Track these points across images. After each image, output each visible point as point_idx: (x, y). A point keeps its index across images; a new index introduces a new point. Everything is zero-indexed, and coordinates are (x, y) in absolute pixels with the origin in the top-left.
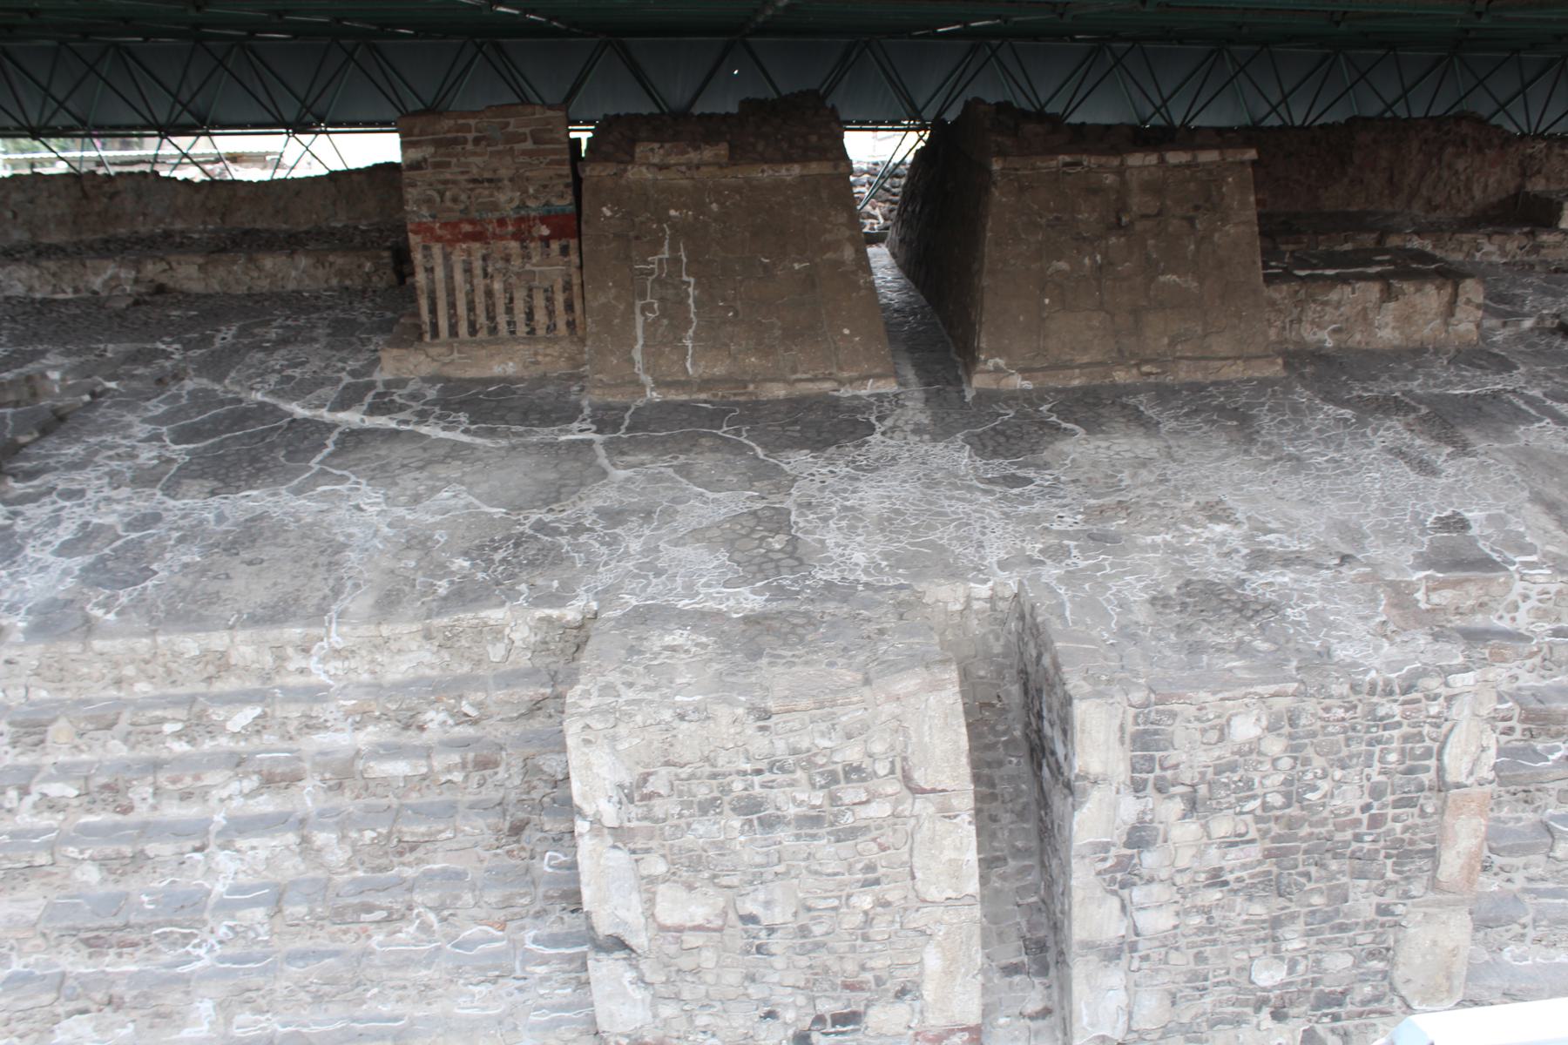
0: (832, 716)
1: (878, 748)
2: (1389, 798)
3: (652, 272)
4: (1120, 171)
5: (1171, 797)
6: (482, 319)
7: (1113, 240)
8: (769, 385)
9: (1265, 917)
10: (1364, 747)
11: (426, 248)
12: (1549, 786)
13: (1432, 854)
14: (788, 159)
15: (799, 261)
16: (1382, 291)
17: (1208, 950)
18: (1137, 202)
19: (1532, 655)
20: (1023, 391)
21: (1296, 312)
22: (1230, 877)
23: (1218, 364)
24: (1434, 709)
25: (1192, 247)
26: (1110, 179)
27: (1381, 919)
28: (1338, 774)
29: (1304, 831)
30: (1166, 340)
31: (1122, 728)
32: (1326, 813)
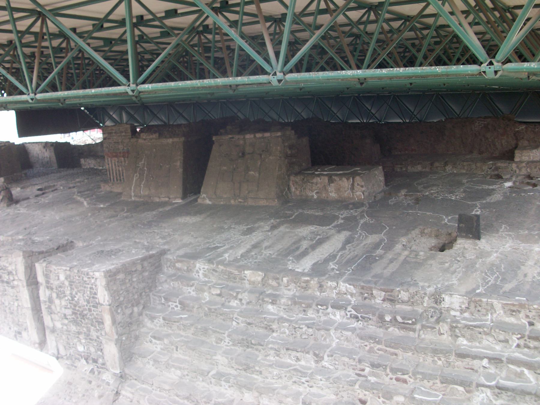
0: (8, 259)
2: (92, 304)
3: (139, 167)
5: (54, 292)
6: (118, 178)
7: (240, 161)
8: (155, 198)
9: (77, 331)
10: (83, 288)
11: (108, 159)
13: (103, 323)
14: (171, 137)
15: (168, 165)
17: (69, 337)
18: (248, 149)
19: (192, 286)
20: (209, 204)
21: (304, 185)
25: (259, 163)
26: (241, 142)
27: (98, 340)
28: (79, 294)
29: (77, 308)
30: (247, 192)
31: (43, 272)
32: (80, 305)
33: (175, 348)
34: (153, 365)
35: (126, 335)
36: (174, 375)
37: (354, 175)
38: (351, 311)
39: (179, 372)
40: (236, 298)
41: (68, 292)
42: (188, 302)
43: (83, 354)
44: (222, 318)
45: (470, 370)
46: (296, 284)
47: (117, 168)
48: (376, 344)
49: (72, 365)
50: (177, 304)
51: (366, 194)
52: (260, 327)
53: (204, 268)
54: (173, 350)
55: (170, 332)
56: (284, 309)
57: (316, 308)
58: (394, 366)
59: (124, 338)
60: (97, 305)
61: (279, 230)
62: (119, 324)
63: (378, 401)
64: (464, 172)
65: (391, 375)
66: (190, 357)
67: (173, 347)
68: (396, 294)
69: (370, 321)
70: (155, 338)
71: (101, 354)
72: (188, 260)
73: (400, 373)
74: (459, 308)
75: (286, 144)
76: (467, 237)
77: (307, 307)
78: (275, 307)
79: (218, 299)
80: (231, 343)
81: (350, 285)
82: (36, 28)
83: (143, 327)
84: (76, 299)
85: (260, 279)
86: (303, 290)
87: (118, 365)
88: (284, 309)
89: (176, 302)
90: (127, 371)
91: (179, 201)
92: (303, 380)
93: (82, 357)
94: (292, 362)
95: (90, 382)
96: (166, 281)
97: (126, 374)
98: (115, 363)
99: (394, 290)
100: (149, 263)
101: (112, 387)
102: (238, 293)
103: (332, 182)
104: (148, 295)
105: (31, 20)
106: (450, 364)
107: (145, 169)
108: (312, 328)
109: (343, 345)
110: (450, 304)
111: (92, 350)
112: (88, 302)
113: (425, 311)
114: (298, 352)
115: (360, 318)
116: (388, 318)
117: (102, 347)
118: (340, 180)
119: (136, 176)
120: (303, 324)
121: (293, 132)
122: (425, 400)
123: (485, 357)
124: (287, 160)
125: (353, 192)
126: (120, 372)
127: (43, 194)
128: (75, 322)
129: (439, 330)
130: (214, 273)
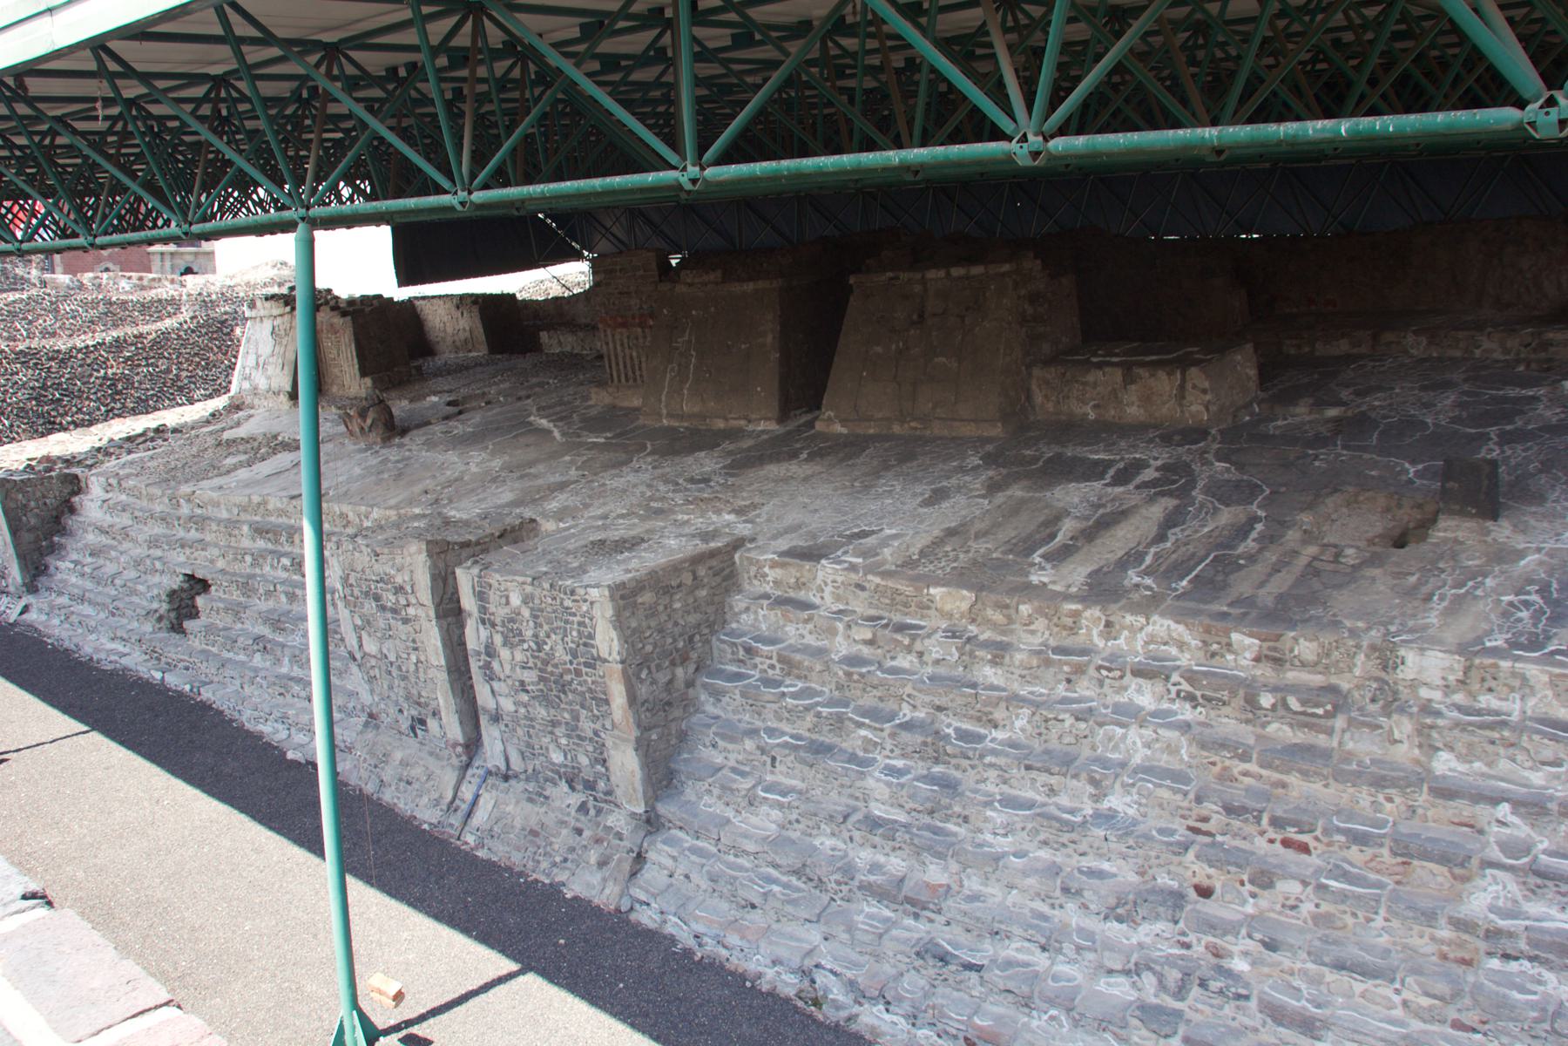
1: (407, 579)
3: (677, 349)
4: (923, 282)
6: (630, 373)
12: (768, 705)
13: (607, 702)
14: (750, 279)
16: (1124, 376)
19: (806, 621)
20: (841, 434)
22: (529, 688)
23: (957, 424)
24: (585, 608)
26: (918, 288)
28: (553, 636)
29: (550, 669)
30: (930, 405)
32: (556, 661)
33: (769, 761)
34: (720, 798)
35: (659, 730)
36: (765, 821)
37: (1184, 363)
38: (1179, 684)
39: (776, 814)
40: (909, 649)
41: (529, 633)
42: (798, 657)
43: (562, 770)
44: (878, 694)
45: (1465, 829)
46: (1050, 620)
47: (627, 351)
48: (1236, 762)
49: (540, 795)
50: (774, 661)
51: (1213, 408)
52: (965, 716)
53: (834, 581)
54: (764, 764)
55: (759, 724)
56: (1023, 677)
57: (1096, 674)
58: (1279, 813)
59: (654, 737)
60: (594, 662)
61: (1009, 493)
62: (643, 704)
63: (1239, 892)
64: (1458, 354)
65: (1271, 834)
66: (803, 781)
67: (764, 757)
68: (1288, 645)
69: (1226, 710)
70: (724, 737)
71: (603, 770)
72: (798, 561)
73: (1293, 830)
74: (1441, 683)
75: (1023, 292)
76: (1462, 513)
77: (1075, 673)
78: (1000, 672)
79: (866, 651)
80: (897, 751)
81: (1178, 622)
82: (463, 39)
83: (697, 711)
84: (547, 648)
85: (965, 606)
86: (1065, 633)
87: (640, 795)
88: (1023, 677)
89: (771, 658)
90: (662, 808)
91: (772, 426)
92: (1065, 838)
93: (560, 778)
94: (1038, 798)
95: (579, 832)
96: (747, 609)
97: (658, 816)
98: (634, 790)
99: (1281, 635)
100: (710, 568)
101: (626, 844)
102: (913, 638)
103: (1132, 382)
104: (708, 642)
105: (451, 21)
106: (1414, 811)
107: (693, 353)
108: (1085, 720)
109: (1159, 761)
110: (1419, 672)
111: (584, 761)
112: (575, 655)
113: (1358, 687)
114: (1052, 774)
115: (1201, 701)
116: (1266, 700)
117: (605, 755)
118: (1152, 375)
119: (672, 370)
120: (1065, 711)
121: (1038, 261)
122: (1353, 892)
123: (1507, 800)
124: (1024, 329)
125: (1181, 405)
126: (646, 812)
127: (460, 413)
128: (544, 699)
129: (1391, 732)
130: (860, 593)
